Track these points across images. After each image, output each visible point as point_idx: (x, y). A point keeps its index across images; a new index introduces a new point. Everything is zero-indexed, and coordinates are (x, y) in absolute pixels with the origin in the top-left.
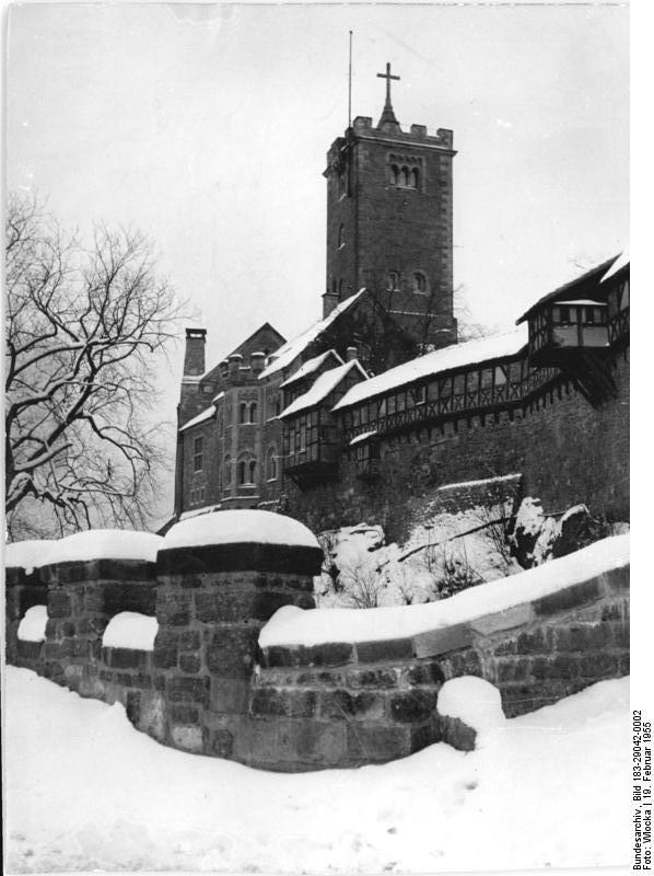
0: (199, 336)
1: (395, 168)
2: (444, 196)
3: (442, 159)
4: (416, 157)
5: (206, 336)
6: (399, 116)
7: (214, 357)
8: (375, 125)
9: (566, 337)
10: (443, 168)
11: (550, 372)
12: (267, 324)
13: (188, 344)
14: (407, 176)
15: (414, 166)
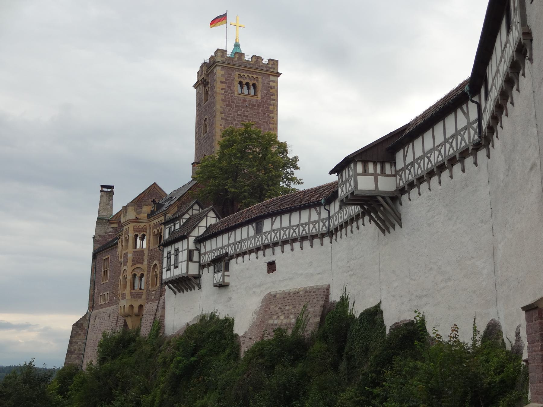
0: (109, 190)
1: (240, 83)
2: (272, 102)
3: (272, 78)
4: (255, 76)
5: (115, 190)
6: (243, 50)
7: (118, 204)
8: (229, 54)
9: (365, 184)
10: (272, 84)
11: (353, 210)
12: (154, 186)
13: (102, 196)
14: (249, 89)
15: (253, 82)
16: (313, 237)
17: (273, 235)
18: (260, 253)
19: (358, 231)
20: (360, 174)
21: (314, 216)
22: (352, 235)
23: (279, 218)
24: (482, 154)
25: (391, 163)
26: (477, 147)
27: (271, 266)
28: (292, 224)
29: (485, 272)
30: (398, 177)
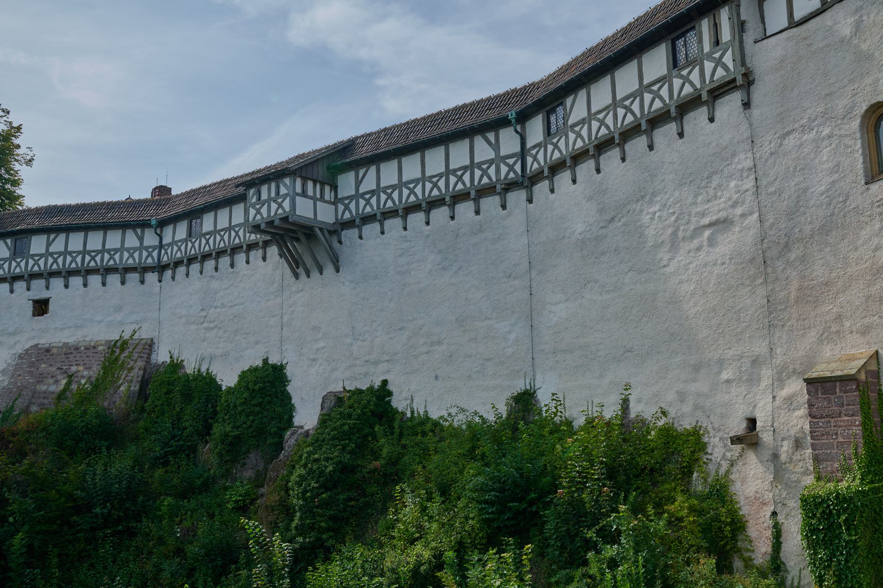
9: (304, 209)
16: (128, 270)
17: (50, 260)
18: (20, 286)
19: (231, 270)
20: (298, 194)
21: (131, 240)
22: (215, 274)
23: (62, 237)
24: (517, 197)
25: (331, 186)
26: (510, 186)
27: (41, 307)
28: (88, 248)
29: (513, 336)
30: (341, 207)
